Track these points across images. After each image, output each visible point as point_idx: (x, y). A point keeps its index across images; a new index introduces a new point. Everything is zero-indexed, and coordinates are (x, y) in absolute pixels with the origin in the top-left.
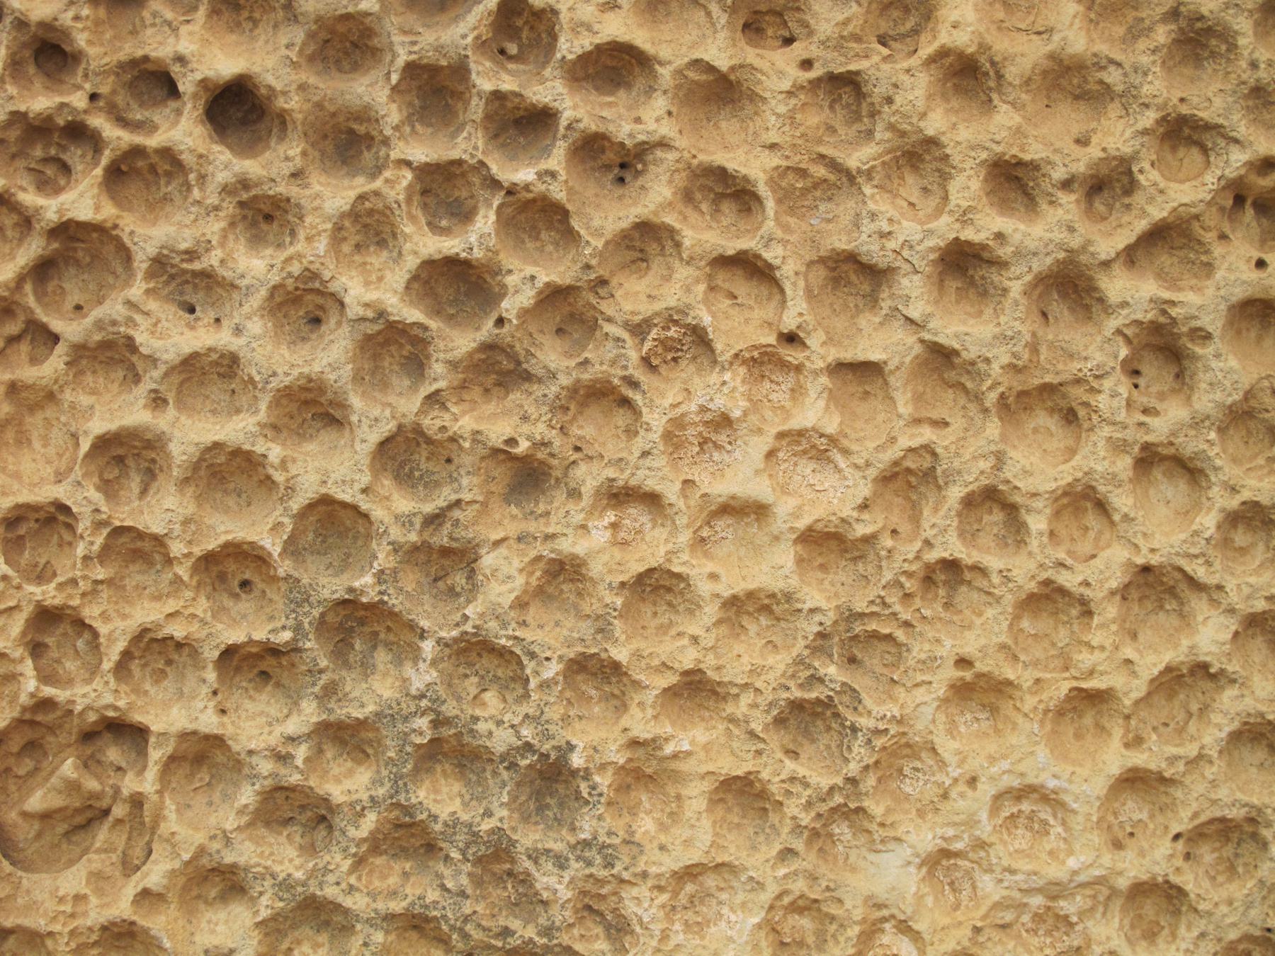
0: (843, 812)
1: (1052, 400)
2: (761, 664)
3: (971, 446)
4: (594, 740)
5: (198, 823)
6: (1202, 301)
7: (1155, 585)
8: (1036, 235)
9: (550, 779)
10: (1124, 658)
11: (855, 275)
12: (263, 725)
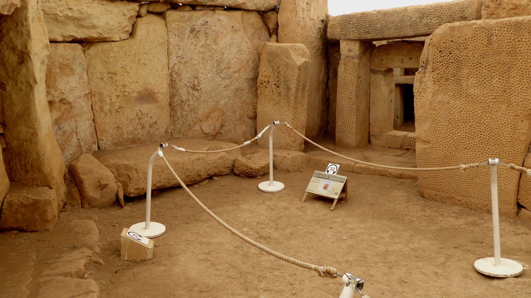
0: (468, 81)
1: (473, 69)
2: (466, 77)
3: (472, 70)
4: (461, 79)
5: (451, 81)
6: (478, 66)
7: (477, 74)
8: (473, 65)
9: (460, 80)
10: (476, 76)
11: (468, 66)
12: (453, 78)
